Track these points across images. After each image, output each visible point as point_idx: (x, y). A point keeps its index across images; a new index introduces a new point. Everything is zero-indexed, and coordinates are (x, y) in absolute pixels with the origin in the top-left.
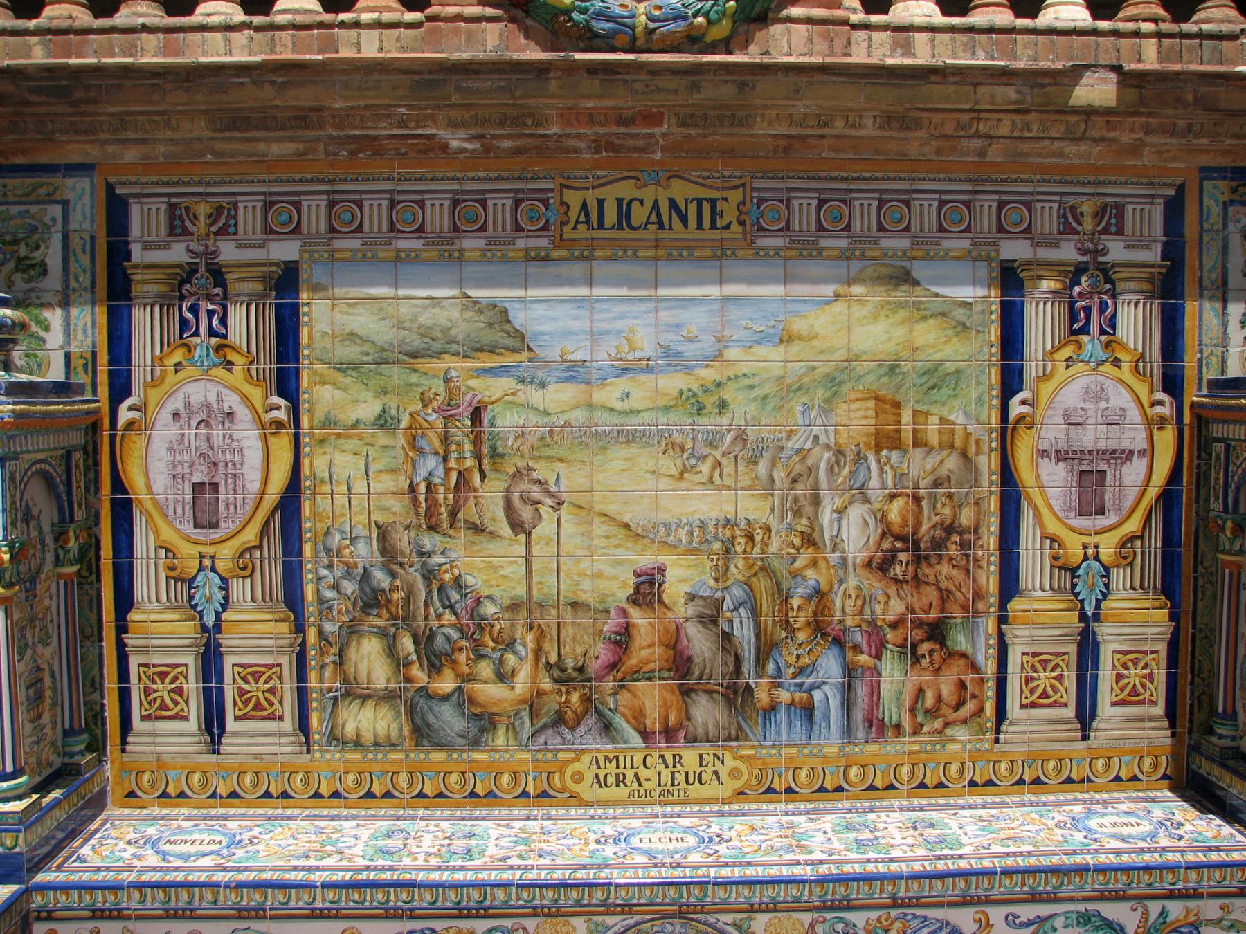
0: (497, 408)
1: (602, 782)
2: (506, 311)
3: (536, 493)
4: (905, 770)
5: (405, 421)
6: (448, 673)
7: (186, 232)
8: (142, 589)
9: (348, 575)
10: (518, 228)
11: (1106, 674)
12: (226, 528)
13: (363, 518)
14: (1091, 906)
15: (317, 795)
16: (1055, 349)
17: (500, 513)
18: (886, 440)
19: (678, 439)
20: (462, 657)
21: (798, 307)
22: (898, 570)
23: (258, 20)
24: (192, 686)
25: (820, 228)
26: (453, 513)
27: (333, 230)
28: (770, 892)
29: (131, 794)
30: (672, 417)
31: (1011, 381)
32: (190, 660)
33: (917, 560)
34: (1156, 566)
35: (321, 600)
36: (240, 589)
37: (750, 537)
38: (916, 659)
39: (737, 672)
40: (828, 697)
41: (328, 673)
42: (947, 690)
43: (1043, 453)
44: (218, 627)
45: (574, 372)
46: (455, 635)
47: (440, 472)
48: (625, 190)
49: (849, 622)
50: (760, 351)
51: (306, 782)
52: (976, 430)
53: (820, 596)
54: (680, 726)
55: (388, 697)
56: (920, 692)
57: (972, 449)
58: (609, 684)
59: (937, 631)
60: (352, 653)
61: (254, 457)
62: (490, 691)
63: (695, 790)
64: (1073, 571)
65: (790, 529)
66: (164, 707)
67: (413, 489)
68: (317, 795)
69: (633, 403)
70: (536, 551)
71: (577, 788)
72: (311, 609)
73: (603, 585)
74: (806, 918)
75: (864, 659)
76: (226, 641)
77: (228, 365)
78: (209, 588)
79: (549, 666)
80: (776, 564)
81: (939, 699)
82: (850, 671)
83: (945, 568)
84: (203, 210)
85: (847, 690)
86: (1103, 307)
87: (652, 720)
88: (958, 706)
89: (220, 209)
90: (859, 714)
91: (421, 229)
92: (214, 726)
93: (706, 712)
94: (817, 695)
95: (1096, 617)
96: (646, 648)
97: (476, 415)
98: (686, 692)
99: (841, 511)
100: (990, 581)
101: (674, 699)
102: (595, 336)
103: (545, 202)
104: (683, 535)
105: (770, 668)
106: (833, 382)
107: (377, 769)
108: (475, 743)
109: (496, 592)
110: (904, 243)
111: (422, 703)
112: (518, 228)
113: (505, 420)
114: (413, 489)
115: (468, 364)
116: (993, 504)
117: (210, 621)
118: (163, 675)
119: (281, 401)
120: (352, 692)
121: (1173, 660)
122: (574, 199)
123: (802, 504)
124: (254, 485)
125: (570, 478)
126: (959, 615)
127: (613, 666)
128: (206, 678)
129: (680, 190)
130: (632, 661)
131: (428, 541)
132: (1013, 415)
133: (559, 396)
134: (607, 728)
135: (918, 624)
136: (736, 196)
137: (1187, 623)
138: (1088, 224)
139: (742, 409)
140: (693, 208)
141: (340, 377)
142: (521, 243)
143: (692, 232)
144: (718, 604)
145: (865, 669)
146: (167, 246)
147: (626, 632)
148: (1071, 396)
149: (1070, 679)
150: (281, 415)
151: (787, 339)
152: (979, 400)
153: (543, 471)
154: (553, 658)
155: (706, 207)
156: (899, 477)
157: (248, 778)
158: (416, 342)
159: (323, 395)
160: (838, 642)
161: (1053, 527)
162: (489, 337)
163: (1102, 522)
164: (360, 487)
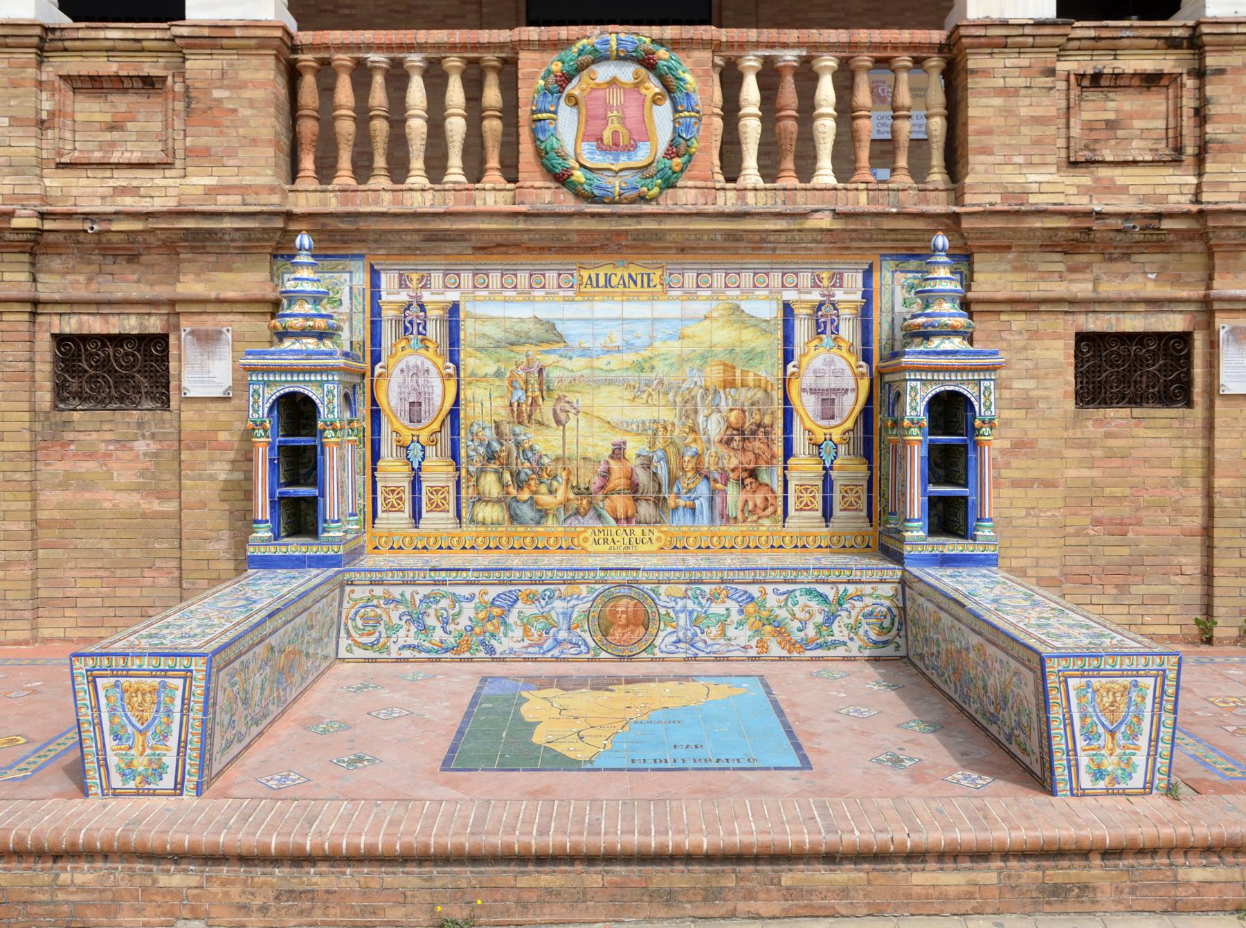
0: (550, 369)
1: (596, 542)
2: (554, 325)
3: (567, 407)
4: (739, 539)
5: (508, 374)
6: (526, 490)
7: (407, 287)
8: (384, 451)
9: (481, 444)
10: (560, 287)
11: (837, 496)
12: (424, 423)
13: (488, 419)
14: (812, 586)
15: (464, 548)
16: (809, 342)
17: (551, 417)
18: (729, 384)
19: (632, 383)
20: (533, 483)
21: (688, 322)
22: (734, 444)
23: (437, 187)
24: (407, 496)
25: (698, 286)
26: (530, 416)
27: (475, 287)
28: (667, 574)
29: (376, 548)
30: (630, 373)
31: (788, 357)
32: (406, 485)
33: (744, 440)
34: (861, 444)
35: (468, 456)
36: (430, 451)
37: (665, 428)
38: (744, 486)
39: (660, 491)
40: (702, 504)
41: (470, 490)
42: (759, 501)
43: (804, 390)
44: (420, 469)
45: (585, 352)
46: (530, 472)
47: (524, 397)
48: (609, 270)
49: (712, 468)
50: (670, 343)
51: (459, 542)
52: (772, 380)
53: (698, 456)
54: (633, 516)
55: (499, 501)
56: (746, 502)
57: (769, 389)
58: (600, 496)
59: (753, 474)
60: (482, 480)
61: (438, 390)
62: (545, 499)
63: (641, 547)
64: (819, 446)
65: (684, 424)
66: (393, 506)
67: (511, 405)
68: (464, 548)
69: (611, 367)
70: (567, 433)
71: (585, 545)
72: (463, 460)
73: (598, 450)
74: (683, 587)
75: (719, 486)
76: (422, 474)
77: (427, 348)
78: (416, 451)
79: (573, 487)
80: (677, 441)
81: (755, 506)
82: (713, 491)
83: (757, 444)
84: (415, 277)
85: (712, 499)
86: (832, 322)
87: (620, 514)
88: (764, 509)
89: (423, 277)
90: (717, 512)
91: (515, 287)
92: (416, 515)
93: (645, 510)
94: (697, 502)
95: (831, 468)
96: (617, 480)
97: (540, 371)
98: (636, 500)
99: (707, 417)
100: (779, 449)
101: (630, 503)
102: (594, 336)
103: (572, 275)
104: (634, 427)
105: (675, 489)
106: (703, 357)
107: (492, 535)
108: (538, 523)
109: (549, 453)
110: (737, 292)
111: (514, 504)
112: (560, 287)
113: (553, 374)
114: (511, 405)
115: (538, 348)
116: (780, 414)
117: (416, 466)
118: (393, 491)
119: (451, 365)
120: (481, 499)
121: (870, 489)
122: (585, 274)
123: (689, 410)
124: (437, 401)
125: (582, 400)
126: (764, 466)
127: (602, 487)
128: (414, 493)
129: (634, 270)
130: (611, 486)
131: (518, 429)
132: (789, 372)
133: (578, 363)
134: (600, 517)
135: (745, 470)
136: (659, 272)
137: (876, 473)
138: (826, 282)
139: (661, 369)
140: (639, 277)
141: (478, 354)
142: (561, 294)
143: (639, 289)
144: (650, 459)
145: (720, 491)
146: (398, 293)
147: (608, 471)
148: (817, 363)
149: (819, 496)
150: (451, 371)
151: (682, 337)
152: (773, 365)
153: (570, 397)
154: (575, 484)
155: (645, 277)
156: (735, 401)
157: (432, 540)
158: (513, 338)
159: (470, 362)
160: (707, 477)
161: (809, 425)
162: (546, 336)
163: (833, 423)
164: (487, 404)
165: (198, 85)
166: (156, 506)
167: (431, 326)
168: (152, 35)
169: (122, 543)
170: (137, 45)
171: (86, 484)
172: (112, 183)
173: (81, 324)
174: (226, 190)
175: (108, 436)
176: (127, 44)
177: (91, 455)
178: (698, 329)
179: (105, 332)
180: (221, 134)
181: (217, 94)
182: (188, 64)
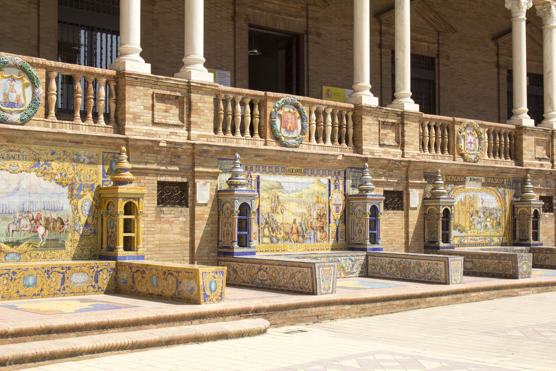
18: (318, 202)
31: (329, 195)
40: (312, 237)
45: (288, 192)
53: (311, 223)
55: (268, 236)
59: (323, 228)
62: (279, 236)
82: (314, 233)
93: (301, 239)
96: (295, 231)
100: (328, 221)
106: (312, 194)
113: (281, 198)
122: (287, 168)
125: (287, 206)
131: (273, 215)
133: (286, 195)
134: (291, 241)
147: (292, 227)
148: (335, 197)
151: (308, 188)
162: (280, 187)
167: (253, 182)
169: (176, 252)
170: (177, 86)
171: (166, 232)
174: (203, 136)
175: (173, 216)
177: (167, 222)
178: (311, 186)
180: (200, 118)
181: (199, 104)
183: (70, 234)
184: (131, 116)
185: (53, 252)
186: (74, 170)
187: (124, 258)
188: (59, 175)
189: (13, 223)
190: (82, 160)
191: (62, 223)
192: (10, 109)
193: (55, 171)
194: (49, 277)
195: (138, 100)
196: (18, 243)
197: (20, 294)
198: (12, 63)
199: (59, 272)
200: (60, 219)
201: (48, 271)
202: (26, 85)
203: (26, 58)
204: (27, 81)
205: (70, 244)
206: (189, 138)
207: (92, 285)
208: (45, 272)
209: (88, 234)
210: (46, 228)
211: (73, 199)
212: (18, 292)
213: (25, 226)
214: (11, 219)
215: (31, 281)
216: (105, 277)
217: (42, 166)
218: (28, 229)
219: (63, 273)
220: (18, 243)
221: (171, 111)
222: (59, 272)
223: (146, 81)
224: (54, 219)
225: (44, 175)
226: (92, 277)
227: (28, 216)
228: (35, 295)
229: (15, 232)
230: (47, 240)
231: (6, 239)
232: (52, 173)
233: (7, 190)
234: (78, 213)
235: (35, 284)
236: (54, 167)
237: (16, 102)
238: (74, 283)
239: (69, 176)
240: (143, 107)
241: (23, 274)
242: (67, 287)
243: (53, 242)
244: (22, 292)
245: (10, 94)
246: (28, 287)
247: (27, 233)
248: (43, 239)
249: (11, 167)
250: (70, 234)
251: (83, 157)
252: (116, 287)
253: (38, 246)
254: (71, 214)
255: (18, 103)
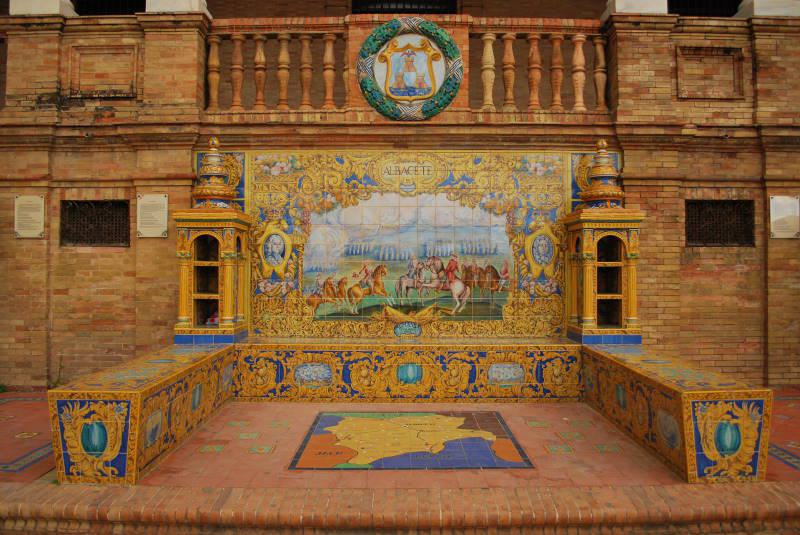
165: (763, 53)
166: (747, 305)
168: (735, 24)
172: (711, 110)
173: (704, 193)
174: (785, 115)
176: (719, 29)
177: (709, 273)
179: (717, 198)
180: (778, 83)
182: (757, 41)
183: (511, 294)
184: (629, 90)
185: (480, 323)
186: (517, 186)
187: (596, 340)
188: (488, 196)
189: (408, 275)
190: (531, 169)
191: (496, 276)
192: (407, 97)
193: (480, 191)
194: (444, 368)
195: (643, 62)
196: (413, 308)
197: (393, 393)
198: (407, 26)
199: (464, 361)
200: (491, 269)
201: (443, 357)
202: (435, 58)
203: (433, 17)
204: (434, 48)
205: (512, 311)
206: (754, 118)
207: (531, 386)
208: (437, 359)
209: (546, 294)
210: (466, 284)
211: (516, 236)
212: (388, 390)
213: (428, 281)
214: (405, 270)
215: (411, 372)
216: (556, 372)
217: (457, 183)
218: (433, 285)
219: (471, 362)
220: (413, 308)
221: (715, 76)
222: (464, 361)
223: (657, 26)
224: (481, 269)
225: (461, 197)
226: (531, 371)
227: (434, 264)
228: (419, 396)
229: (411, 290)
230: (469, 303)
231: (396, 300)
232: (475, 194)
233: (397, 223)
234: (525, 258)
235: (419, 378)
236: (478, 184)
237: (417, 86)
238: (496, 380)
239: (507, 197)
240: (653, 73)
241: (396, 360)
242: (482, 386)
243: (478, 307)
244: (395, 390)
245: (406, 74)
246: (406, 382)
247: (432, 291)
248: (460, 301)
249: (402, 187)
250: (511, 294)
251: (533, 165)
252: (582, 392)
253: (453, 313)
254: (512, 261)
255: (420, 88)
